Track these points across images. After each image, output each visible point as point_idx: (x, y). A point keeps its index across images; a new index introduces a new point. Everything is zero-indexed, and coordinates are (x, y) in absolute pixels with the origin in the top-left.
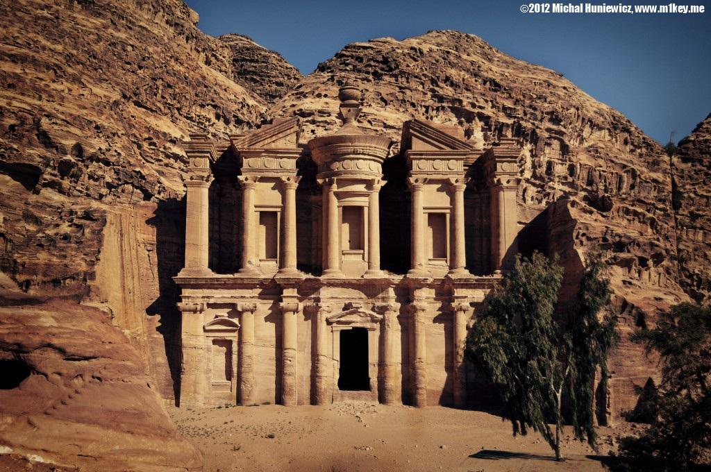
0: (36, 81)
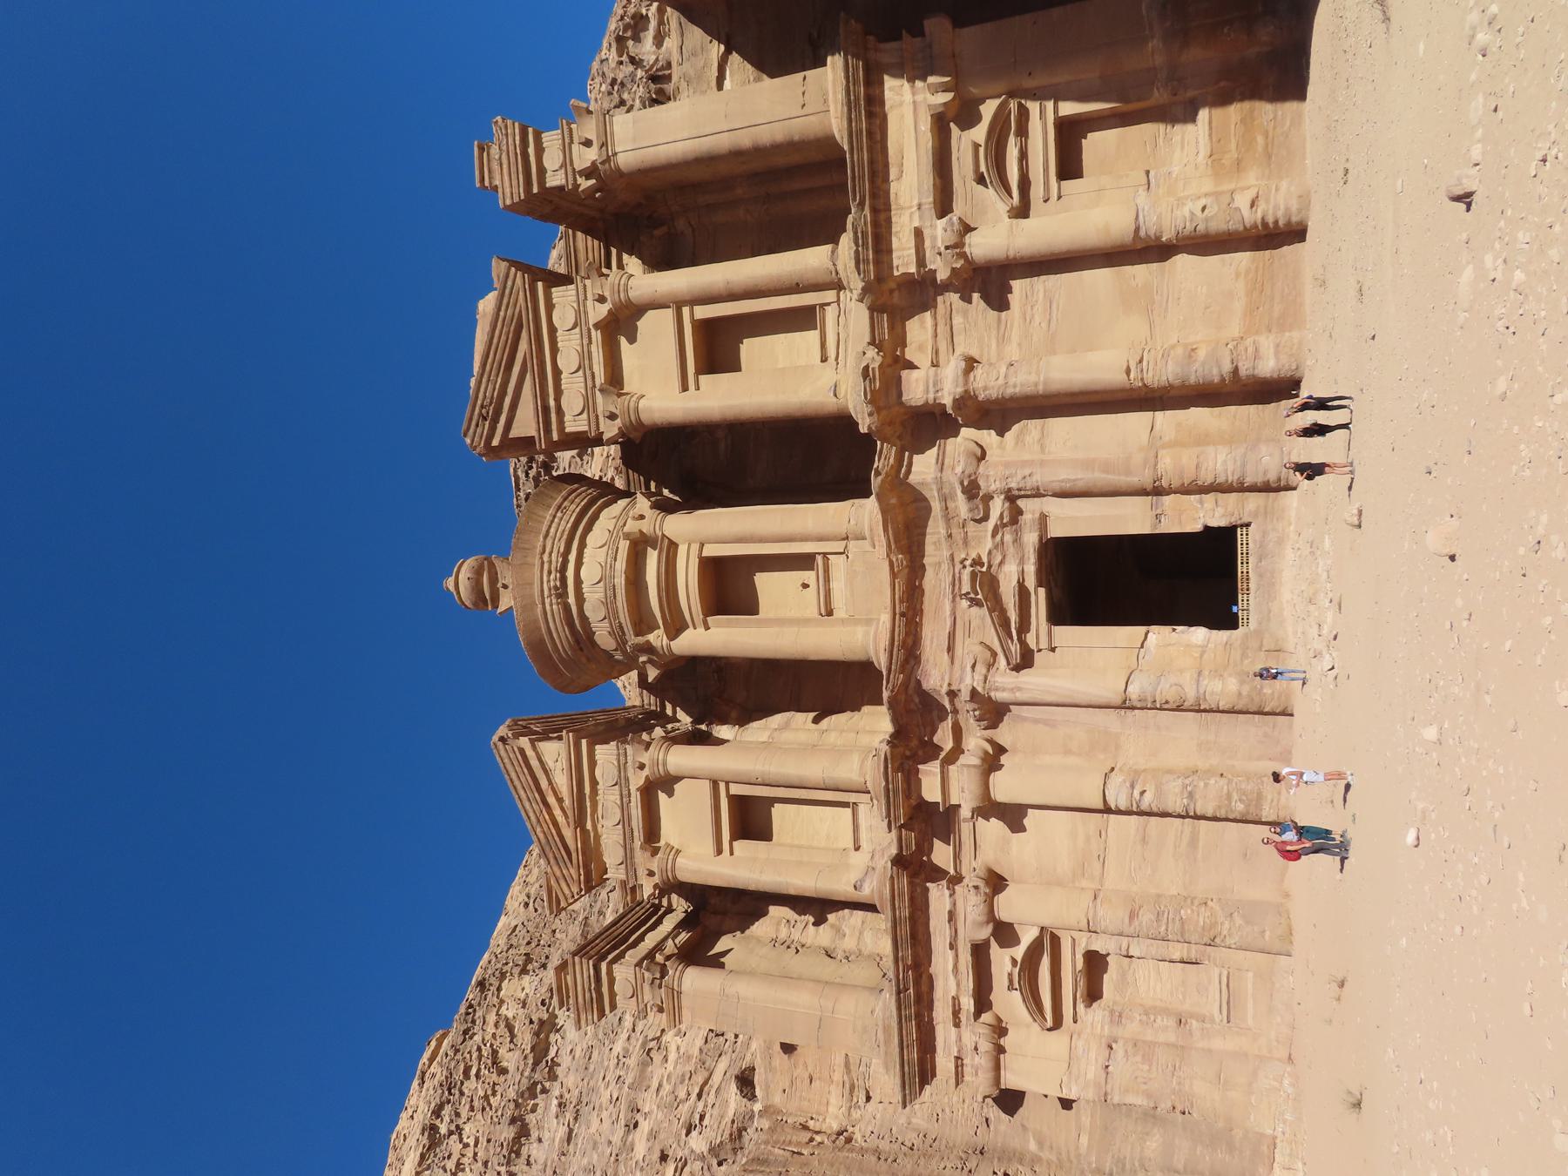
0: (662, 1098)
